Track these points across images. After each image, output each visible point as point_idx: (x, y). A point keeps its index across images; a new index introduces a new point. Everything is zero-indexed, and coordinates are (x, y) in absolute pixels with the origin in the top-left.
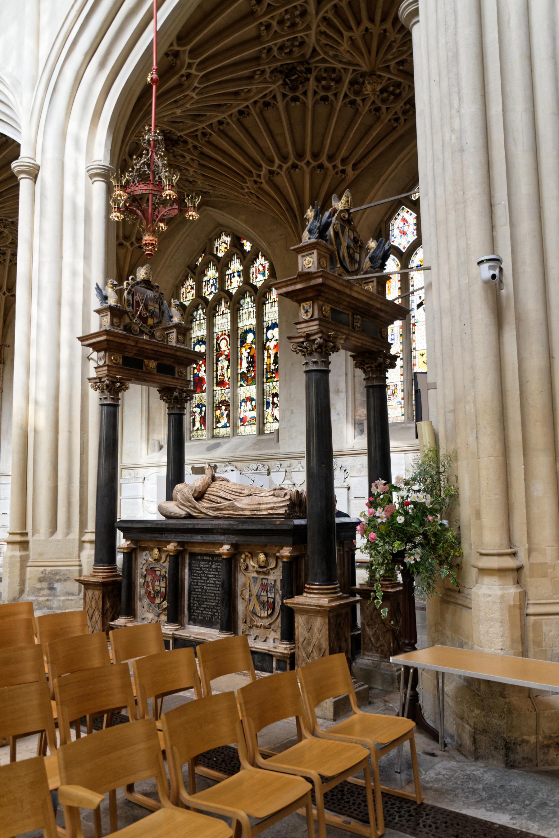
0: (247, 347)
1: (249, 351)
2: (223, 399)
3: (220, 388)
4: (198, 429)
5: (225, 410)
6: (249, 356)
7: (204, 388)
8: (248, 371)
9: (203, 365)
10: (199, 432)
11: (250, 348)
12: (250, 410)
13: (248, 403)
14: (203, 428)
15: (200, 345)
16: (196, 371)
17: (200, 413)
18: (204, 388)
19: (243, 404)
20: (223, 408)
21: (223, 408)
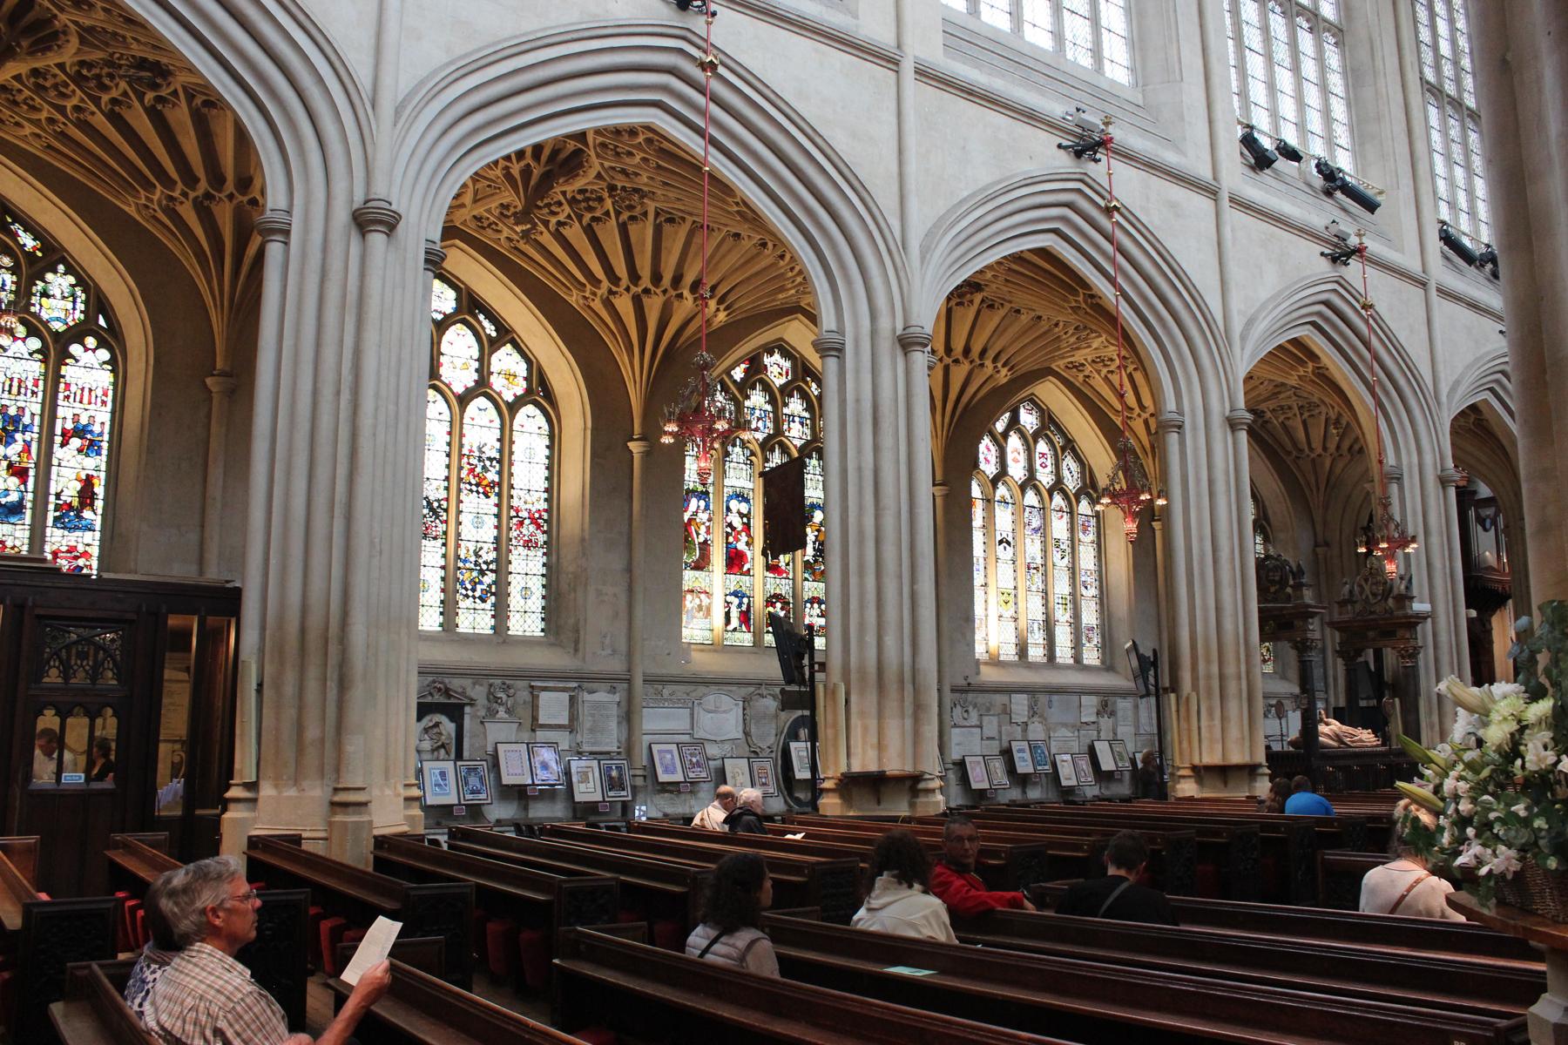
0: (814, 528)
1: (816, 533)
2: (778, 591)
3: (772, 575)
4: (735, 630)
5: (782, 609)
6: (816, 540)
7: (745, 569)
8: (816, 561)
9: (744, 534)
10: (737, 635)
11: (818, 531)
12: (818, 616)
13: (816, 606)
14: (744, 628)
15: (740, 502)
16: (731, 539)
17: (740, 605)
18: (745, 569)
19: (808, 605)
20: (779, 605)
21: (779, 605)
